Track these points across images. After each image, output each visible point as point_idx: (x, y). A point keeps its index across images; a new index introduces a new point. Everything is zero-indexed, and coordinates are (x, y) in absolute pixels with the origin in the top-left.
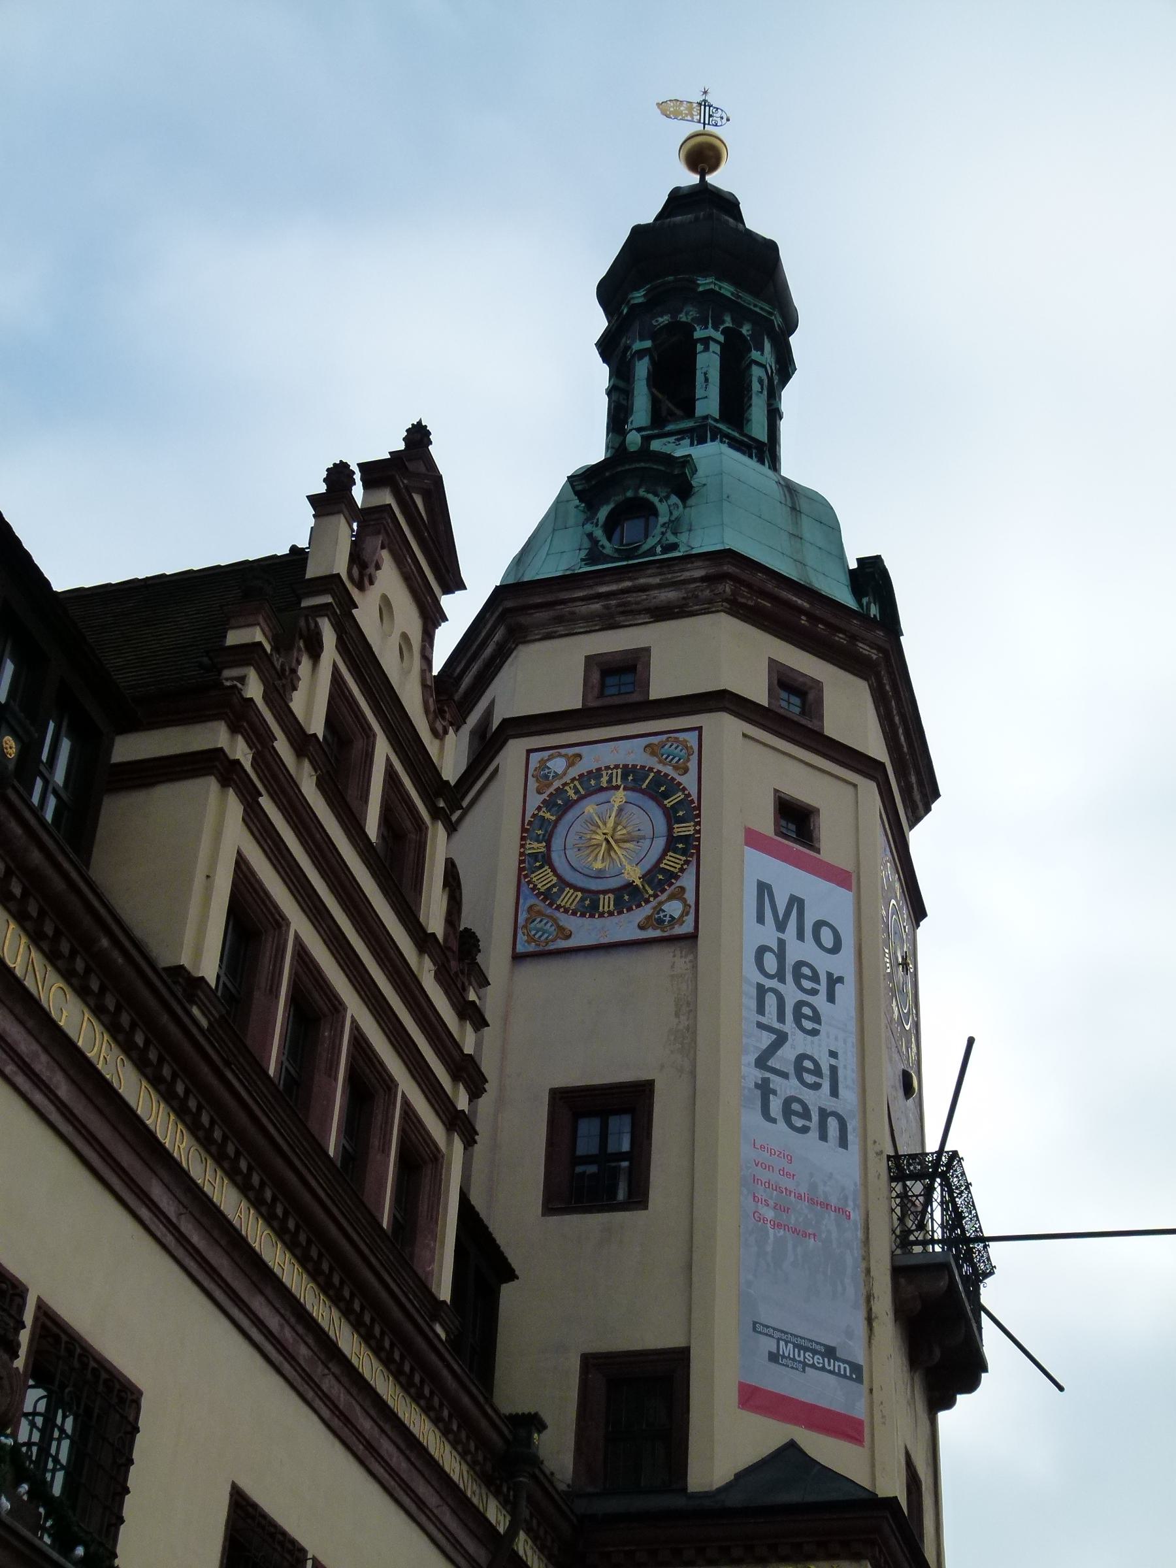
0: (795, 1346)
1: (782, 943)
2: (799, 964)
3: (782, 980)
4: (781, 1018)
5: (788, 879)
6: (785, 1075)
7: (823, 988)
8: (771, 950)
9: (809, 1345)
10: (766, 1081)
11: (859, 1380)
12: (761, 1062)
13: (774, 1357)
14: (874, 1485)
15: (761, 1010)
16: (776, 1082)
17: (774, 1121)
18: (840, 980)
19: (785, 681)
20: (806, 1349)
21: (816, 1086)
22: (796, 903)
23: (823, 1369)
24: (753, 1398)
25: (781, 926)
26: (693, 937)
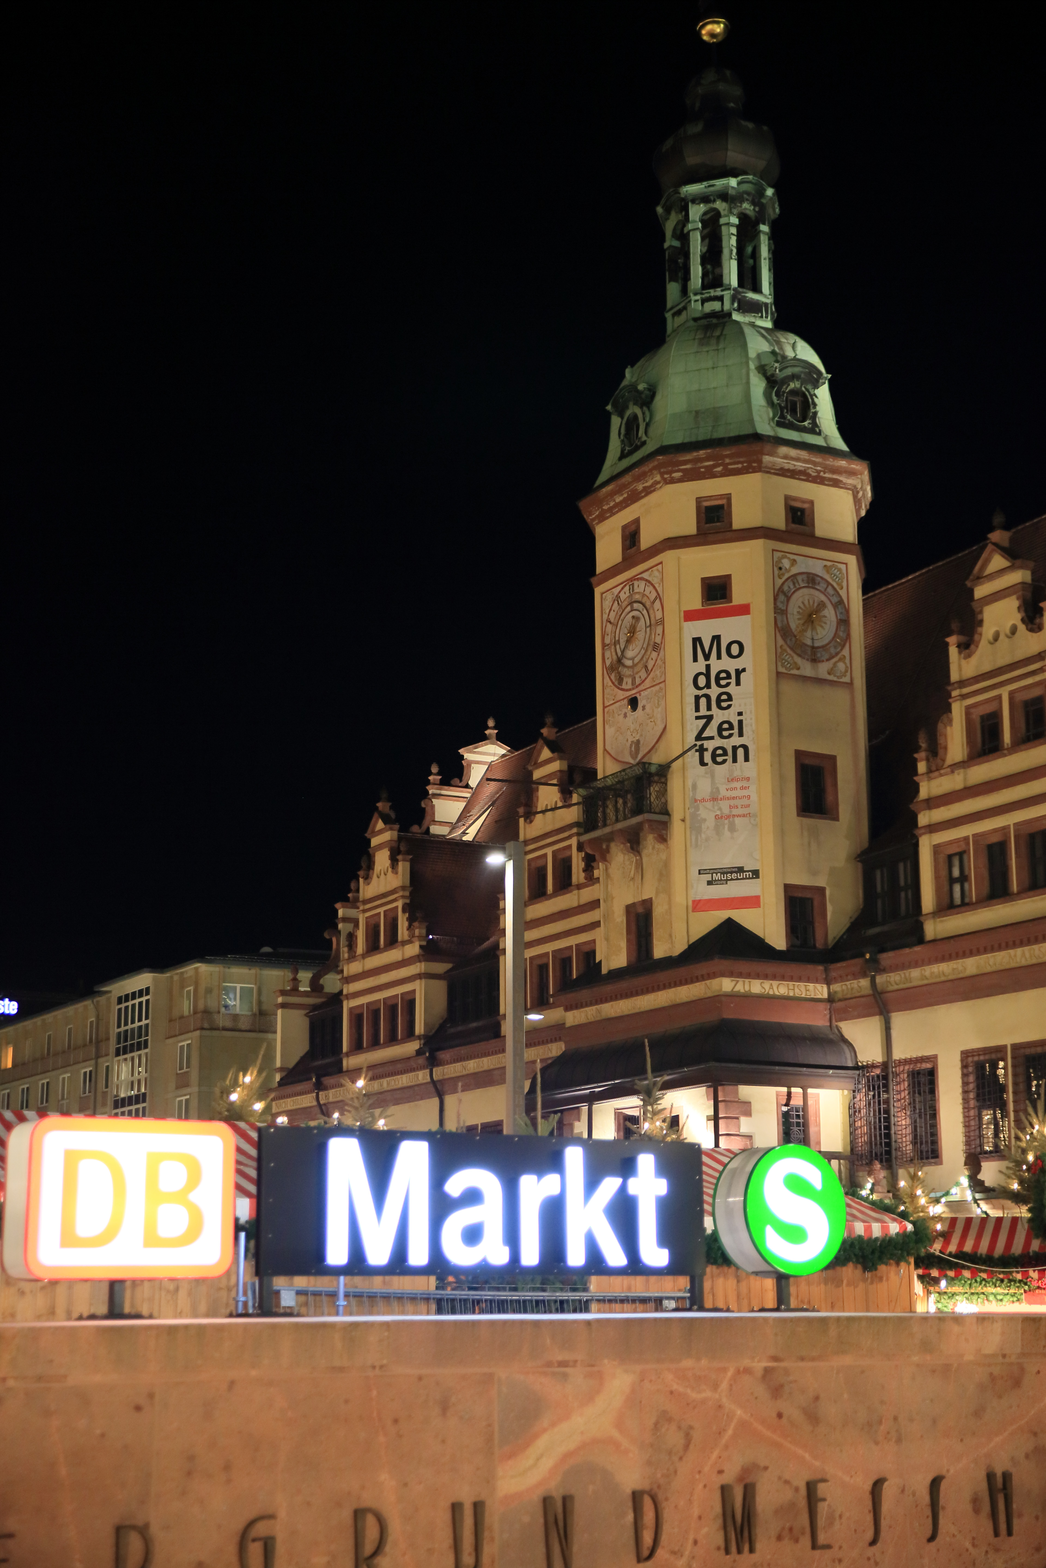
0: (721, 873)
1: (708, 667)
4: (709, 708)
5: (705, 629)
7: (733, 680)
12: (699, 737)
13: (710, 883)
15: (697, 709)
16: (707, 744)
17: (706, 764)
18: (744, 670)
20: (727, 873)
22: (717, 639)
23: (737, 879)
25: (707, 657)
26: (664, 681)
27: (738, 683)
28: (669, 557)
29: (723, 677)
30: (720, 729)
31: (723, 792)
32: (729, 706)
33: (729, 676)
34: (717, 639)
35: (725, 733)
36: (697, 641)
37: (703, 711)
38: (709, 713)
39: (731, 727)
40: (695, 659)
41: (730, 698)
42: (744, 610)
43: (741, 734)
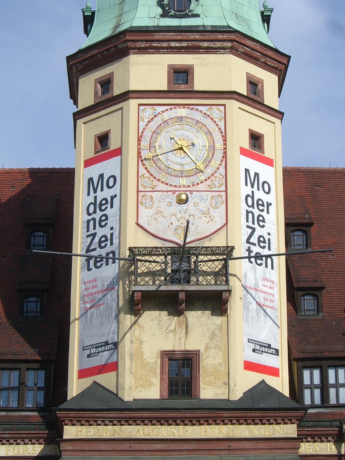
1: (253, 192)
2: (259, 200)
3: (253, 208)
4: (253, 223)
5: (255, 166)
6: (254, 244)
7: (265, 208)
8: (250, 196)
9: (263, 345)
10: (249, 248)
11: (278, 355)
12: (248, 241)
14: (283, 391)
15: (247, 221)
16: (253, 248)
19: (254, 84)
21: (264, 247)
22: (257, 175)
24: (249, 366)
25: (252, 186)
27: (268, 213)
28: (233, 105)
29: (260, 203)
30: (259, 241)
31: (261, 287)
32: (263, 226)
33: (263, 205)
34: (257, 175)
35: (262, 244)
36: (247, 171)
37: (250, 224)
38: (253, 226)
39: (264, 242)
40: (246, 185)
41: (264, 221)
42: (269, 162)
43: (269, 249)
